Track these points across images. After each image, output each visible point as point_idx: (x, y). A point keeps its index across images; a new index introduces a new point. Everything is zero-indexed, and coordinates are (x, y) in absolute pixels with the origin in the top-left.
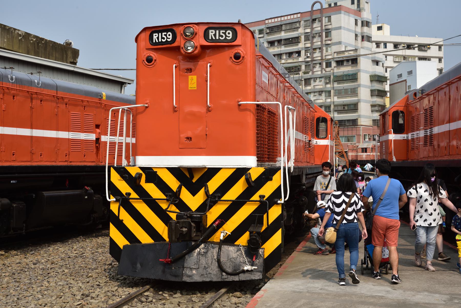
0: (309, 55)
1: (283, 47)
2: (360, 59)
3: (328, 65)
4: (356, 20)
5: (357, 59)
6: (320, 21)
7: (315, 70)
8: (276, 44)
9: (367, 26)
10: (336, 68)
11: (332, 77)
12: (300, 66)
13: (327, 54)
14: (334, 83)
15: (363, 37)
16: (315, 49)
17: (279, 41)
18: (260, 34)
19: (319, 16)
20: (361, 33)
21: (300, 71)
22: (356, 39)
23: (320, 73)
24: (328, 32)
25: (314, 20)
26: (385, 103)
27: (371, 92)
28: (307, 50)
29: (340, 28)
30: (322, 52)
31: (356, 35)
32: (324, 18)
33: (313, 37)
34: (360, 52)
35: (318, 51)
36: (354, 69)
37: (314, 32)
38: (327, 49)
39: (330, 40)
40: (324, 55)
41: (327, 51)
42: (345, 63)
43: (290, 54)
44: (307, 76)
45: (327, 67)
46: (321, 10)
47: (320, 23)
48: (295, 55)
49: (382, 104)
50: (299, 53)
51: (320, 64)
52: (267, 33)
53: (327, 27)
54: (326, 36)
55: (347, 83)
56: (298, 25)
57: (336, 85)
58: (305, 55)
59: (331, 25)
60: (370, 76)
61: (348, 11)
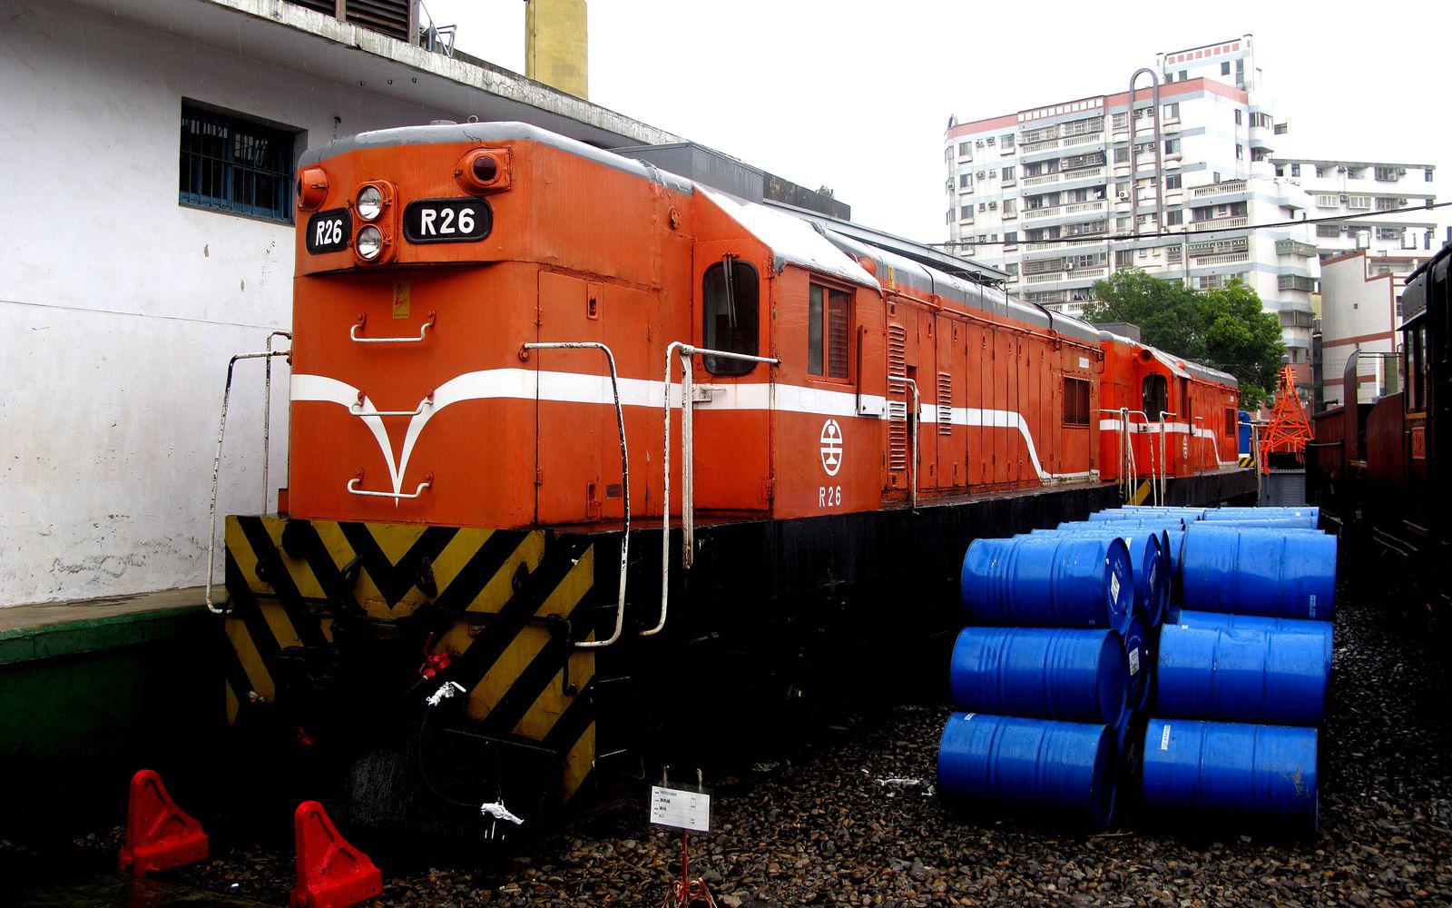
0: (1126, 196)
1: (1062, 176)
3: (1175, 217)
4: (1236, 111)
5: (1245, 203)
6: (1153, 112)
8: (1045, 169)
9: (1263, 125)
11: (1184, 244)
14: (1190, 260)
17: (1052, 163)
19: (1150, 102)
20: (1250, 141)
22: (1238, 156)
25: (1137, 114)
26: (1310, 309)
27: (1280, 282)
29: (1200, 131)
31: (1239, 148)
32: (1161, 107)
33: (1136, 153)
39: (1179, 160)
40: (1164, 195)
42: (1216, 214)
43: (1080, 193)
45: (1171, 222)
46: (1157, 91)
47: (1152, 119)
48: (1091, 196)
49: (1306, 310)
50: (1101, 189)
51: (1154, 215)
52: (1021, 145)
53: (1169, 129)
54: (1169, 151)
55: (1220, 260)
57: (1194, 264)
58: (1117, 195)
59: (1179, 123)
60: (1276, 242)
61: (1219, 90)
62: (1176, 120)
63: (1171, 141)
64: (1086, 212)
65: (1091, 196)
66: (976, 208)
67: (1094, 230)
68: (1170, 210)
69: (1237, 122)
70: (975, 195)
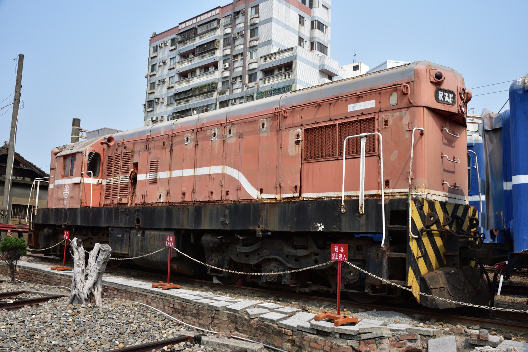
2: (296, 63)
4: (300, 16)
7: (235, 86)
10: (261, 81)
12: (216, 84)
13: (251, 61)
15: (312, 44)
16: (235, 56)
17: (193, 52)
18: (172, 45)
21: (214, 91)
23: (239, 91)
24: (254, 29)
28: (226, 58)
30: (244, 60)
31: (301, 40)
33: (235, 39)
34: (296, 52)
35: (240, 57)
36: (288, 79)
37: (235, 32)
38: (251, 54)
41: (251, 58)
42: (276, 72)
43: (205, 68)
44: (224, 97)
45: (250, 81)
47: (244, 17)
48: (212, 69)
50: (215, 65)
56: (215, 24)
59: (258, 17)
62: (257, 15)
63: (253, 29)
64: (207, 79)
65: (212, 69)
66: (157, 82)
67: (210, 88)
68: (250, 73)
69: (300, 23)
70: (157, 76)
